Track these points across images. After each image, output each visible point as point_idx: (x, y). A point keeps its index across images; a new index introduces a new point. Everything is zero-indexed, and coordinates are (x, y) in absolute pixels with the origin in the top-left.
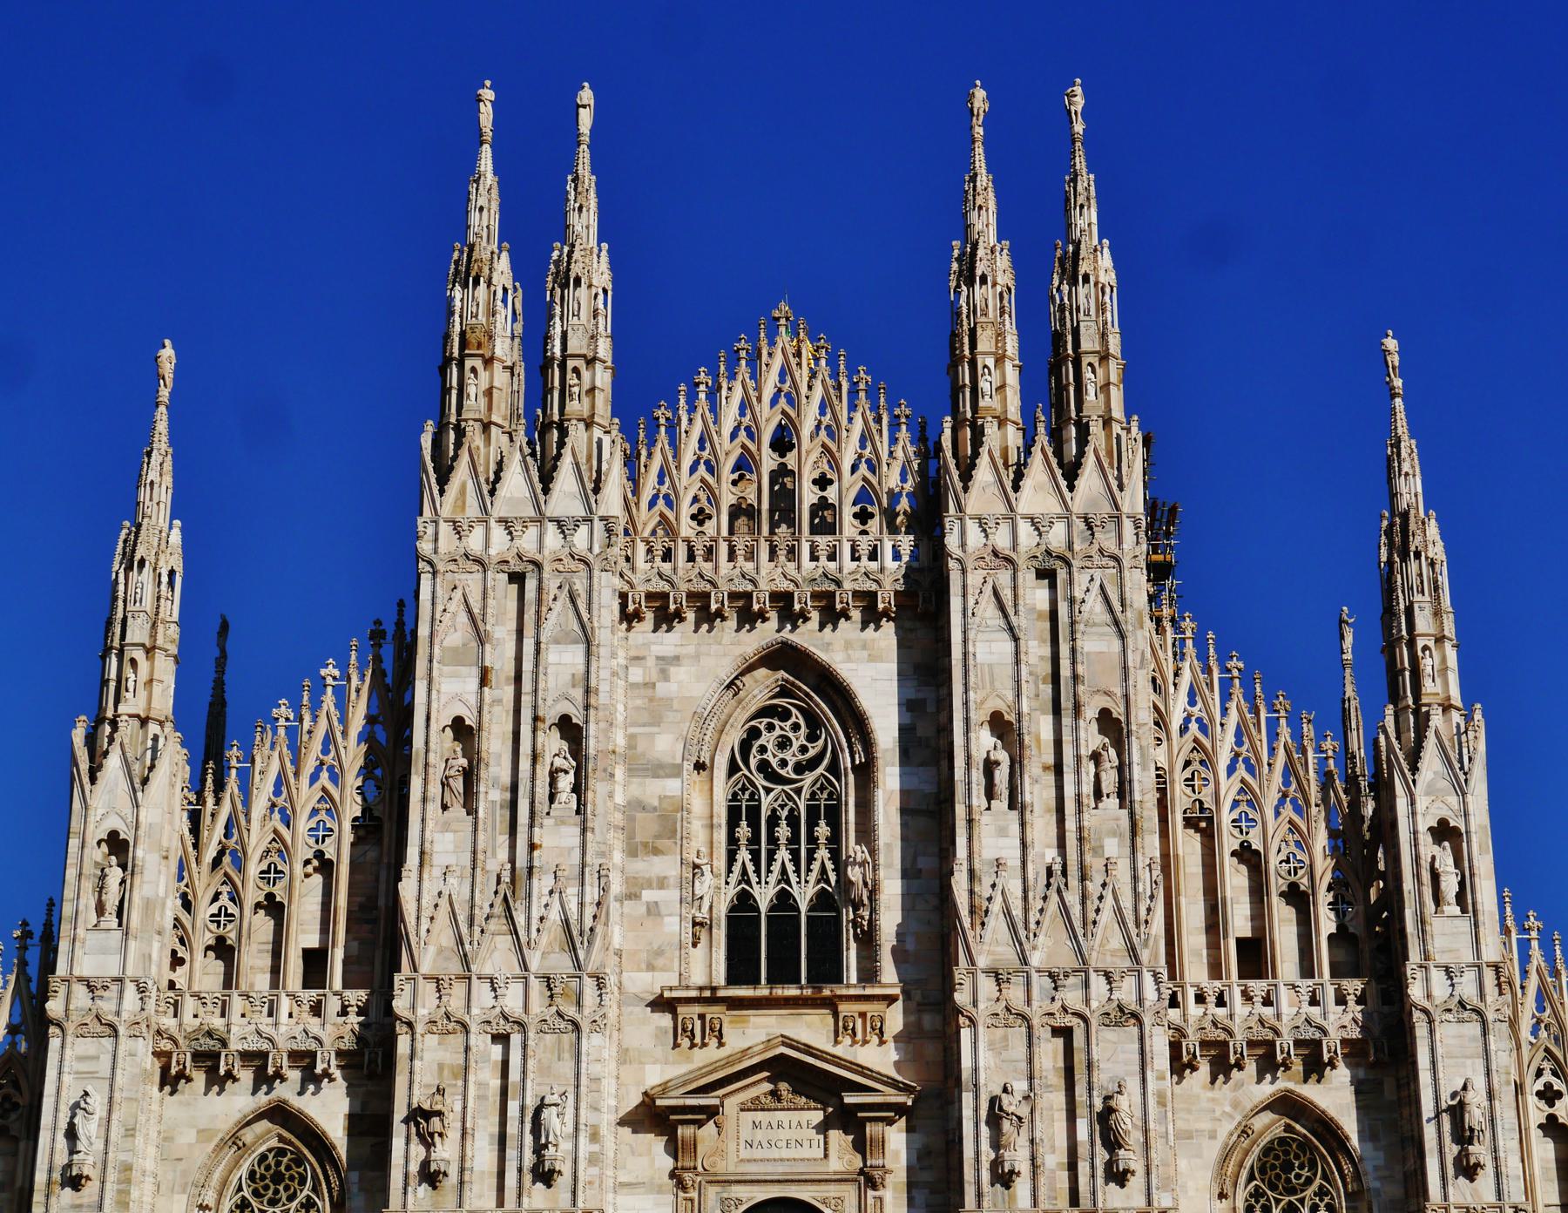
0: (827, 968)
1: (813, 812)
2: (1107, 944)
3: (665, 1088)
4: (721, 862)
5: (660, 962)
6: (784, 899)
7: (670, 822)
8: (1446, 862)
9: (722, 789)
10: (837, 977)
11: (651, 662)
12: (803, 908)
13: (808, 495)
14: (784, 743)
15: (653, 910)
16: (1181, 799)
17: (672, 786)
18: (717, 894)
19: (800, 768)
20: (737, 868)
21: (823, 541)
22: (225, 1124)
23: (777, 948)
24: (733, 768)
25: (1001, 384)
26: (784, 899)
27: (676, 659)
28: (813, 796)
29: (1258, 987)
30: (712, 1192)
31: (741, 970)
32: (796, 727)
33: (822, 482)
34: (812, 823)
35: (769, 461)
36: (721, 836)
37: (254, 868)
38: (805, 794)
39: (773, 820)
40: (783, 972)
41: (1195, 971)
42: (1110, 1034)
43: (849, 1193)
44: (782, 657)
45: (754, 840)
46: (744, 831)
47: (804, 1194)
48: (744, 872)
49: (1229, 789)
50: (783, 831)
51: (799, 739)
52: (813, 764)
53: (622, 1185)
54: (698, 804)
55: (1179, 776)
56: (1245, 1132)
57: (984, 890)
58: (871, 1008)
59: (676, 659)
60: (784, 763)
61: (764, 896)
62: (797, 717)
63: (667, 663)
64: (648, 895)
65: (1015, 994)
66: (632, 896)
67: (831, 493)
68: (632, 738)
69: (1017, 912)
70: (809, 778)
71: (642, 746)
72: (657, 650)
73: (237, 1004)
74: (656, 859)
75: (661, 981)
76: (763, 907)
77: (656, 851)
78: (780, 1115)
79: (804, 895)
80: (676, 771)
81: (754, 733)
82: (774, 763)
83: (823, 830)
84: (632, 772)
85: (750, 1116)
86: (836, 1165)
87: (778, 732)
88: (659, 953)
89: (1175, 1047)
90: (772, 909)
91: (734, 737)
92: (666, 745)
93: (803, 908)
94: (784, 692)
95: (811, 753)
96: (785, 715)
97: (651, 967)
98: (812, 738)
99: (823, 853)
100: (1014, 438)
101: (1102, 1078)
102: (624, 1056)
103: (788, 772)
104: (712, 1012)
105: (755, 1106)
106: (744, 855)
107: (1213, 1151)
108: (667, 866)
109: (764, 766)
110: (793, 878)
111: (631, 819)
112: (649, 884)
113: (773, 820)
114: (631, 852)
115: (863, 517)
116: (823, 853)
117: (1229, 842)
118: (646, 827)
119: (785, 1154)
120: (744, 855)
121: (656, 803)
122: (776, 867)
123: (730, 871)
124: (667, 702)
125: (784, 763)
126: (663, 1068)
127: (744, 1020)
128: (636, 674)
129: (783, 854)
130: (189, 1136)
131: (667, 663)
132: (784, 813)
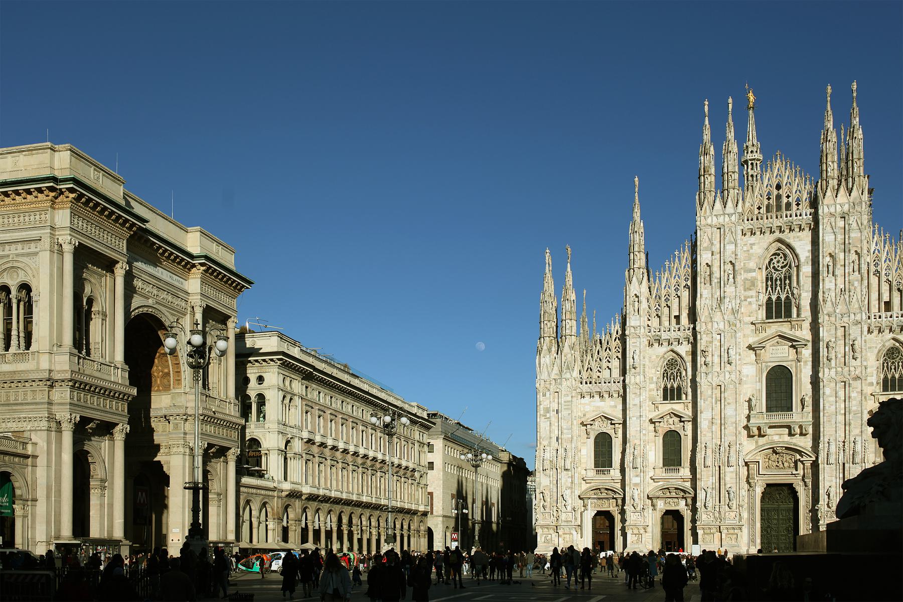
0: (788, 314)
1: (785, 277)
2: (855, 305)
3: (754, 343)
6: (779, 298)
7: (753, 283)
9: (764, 273)
10: (790, 316)
13: (785, 200)
15: (750, 303)
16: (873, 269)
17: (754, 274)
18: (763, 298)
19: (782, 267)
21: (789, 213)
22: (661, 354)
23: (778, 309)
24: (767, 268)
25: (832, 169)
26: (779, 298)
27: (754, 244)
29: (889, 314)
31: (769, 316)
33: (788, 197)
34: (785, 280)
35: (775, 192)
37: (663, 299)
39: (776, 280)
40: (778, 316)
41: (874, 309)
42: (854, 327)
43: (794, 363)
44: (780, 241)
45: (772, 285)
46: (769, 283)
47: (784, 364)
49: (884, 266)
50: (778, 282)
52: (785, 266)
54: (759, 278)
55: (872, 264)
56: (884, 346)
57: (826, 296)
58: (799, 323)
59: (754, 244)
61: (774, 298)
62: (781, 255)
63: (752, 245)
65: (833, 319)
73: (662, 329)
75: (753, 319)
79: (783, 297)
80: (754, 271)
81: (772, 260)
83: (787, 282)
86: (791, 358)
89: (869, 329)
92: (752, 265)
94: (779, 249)
96: (779, 255)
98: (785, 260)
99: (787, 287)
100: (836, 182)
101: (851, 337)
104: (763, 325)
105: (773, 345)
106: (769, 289)
107: (876, 351)
108: (753, 293)
109: (774, 267)
113: (776, 280)
114: (745, 290)
115: (798, 205)
116: (787, 287)
117: (884, 278)
118: (748, 284)
120: (769, 289)
124: (752, 254)
126: (752, 340)
128: (745, 248)
129: (778, 288)
130: (654, 357)
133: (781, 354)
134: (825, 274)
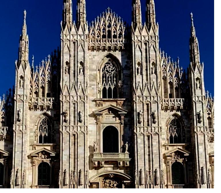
2: (153, 93)
4: (101, 83)
5: (94, 95)
6: (110, 88)
7: (95, 78)
8: (198, 82)
9: (101, 73)
11: (92, 56)
12: (112, 89)
13: (113, 34)
14: (110, 67)
15: (93, 89)
17: (95, 72)
18: (101, 87)
19: (112, 71)
20: (104, 84)
24: (103, 71)
26: (110, 88)
28: (113, 75)
30: (101, 125)
31: (104, 96)
32: (111, 65)
33: (114, 32)
36: (101, 79)
38: (112, 74)
39: (108, 77)
40: (110, 97)
42: (154, 104)
45: (106, 80)
46: (104, 79)
48: (104, 84)
50: (110, 79)
51: (111, 67)
53: (90, 124)
57: (137, 86)
60: (109, 70)
61: (107, 87)
63: (94, 56)
64: (92, 87)
66: (90, 87)
67: (116, 33)
68: (90, 66)
69: (142, 88)
70: (113, 72)
71: (91, 67)
72: (93, 54)
74: (93, 82)
75: (94, 98)
76: (107, 89)
77: (93, 81)
78: (110, 115)
81: (105, 66)
82: (108, 70)
84: (90, 70)
85: (106, 115)
87: (109, 66)
88: (94, 94)
90: (108, 89)
91: (103, 67)
92: (94, 67)
93: (112, 89)
94: (109, 61)
95: (113, 69)
96: (109, 64)
97: (93, 96)
98: (113, 67)
102: (90, 107)
103: (110, 71)
106: (104, 82)
107: (165, 120)
108: (95, 83)
109: (107, 71)
110: (111, 85)
111: (90, 76)
112: (92, 85)
113: (108, 77)
114: (90, 81)
118: (92, 77)
119: (111, 120)
120: (104, 82)
121: (93, 74)
122: (109, 84)
123: (103, 84)
124: (94, 61)
125: (109, 70)
127: (105, 103)
128: (90, 57)
129: (110, 82)
131: (94, 56)
132: (110, 77)
133: (109, 120)
134: (136, 74)
